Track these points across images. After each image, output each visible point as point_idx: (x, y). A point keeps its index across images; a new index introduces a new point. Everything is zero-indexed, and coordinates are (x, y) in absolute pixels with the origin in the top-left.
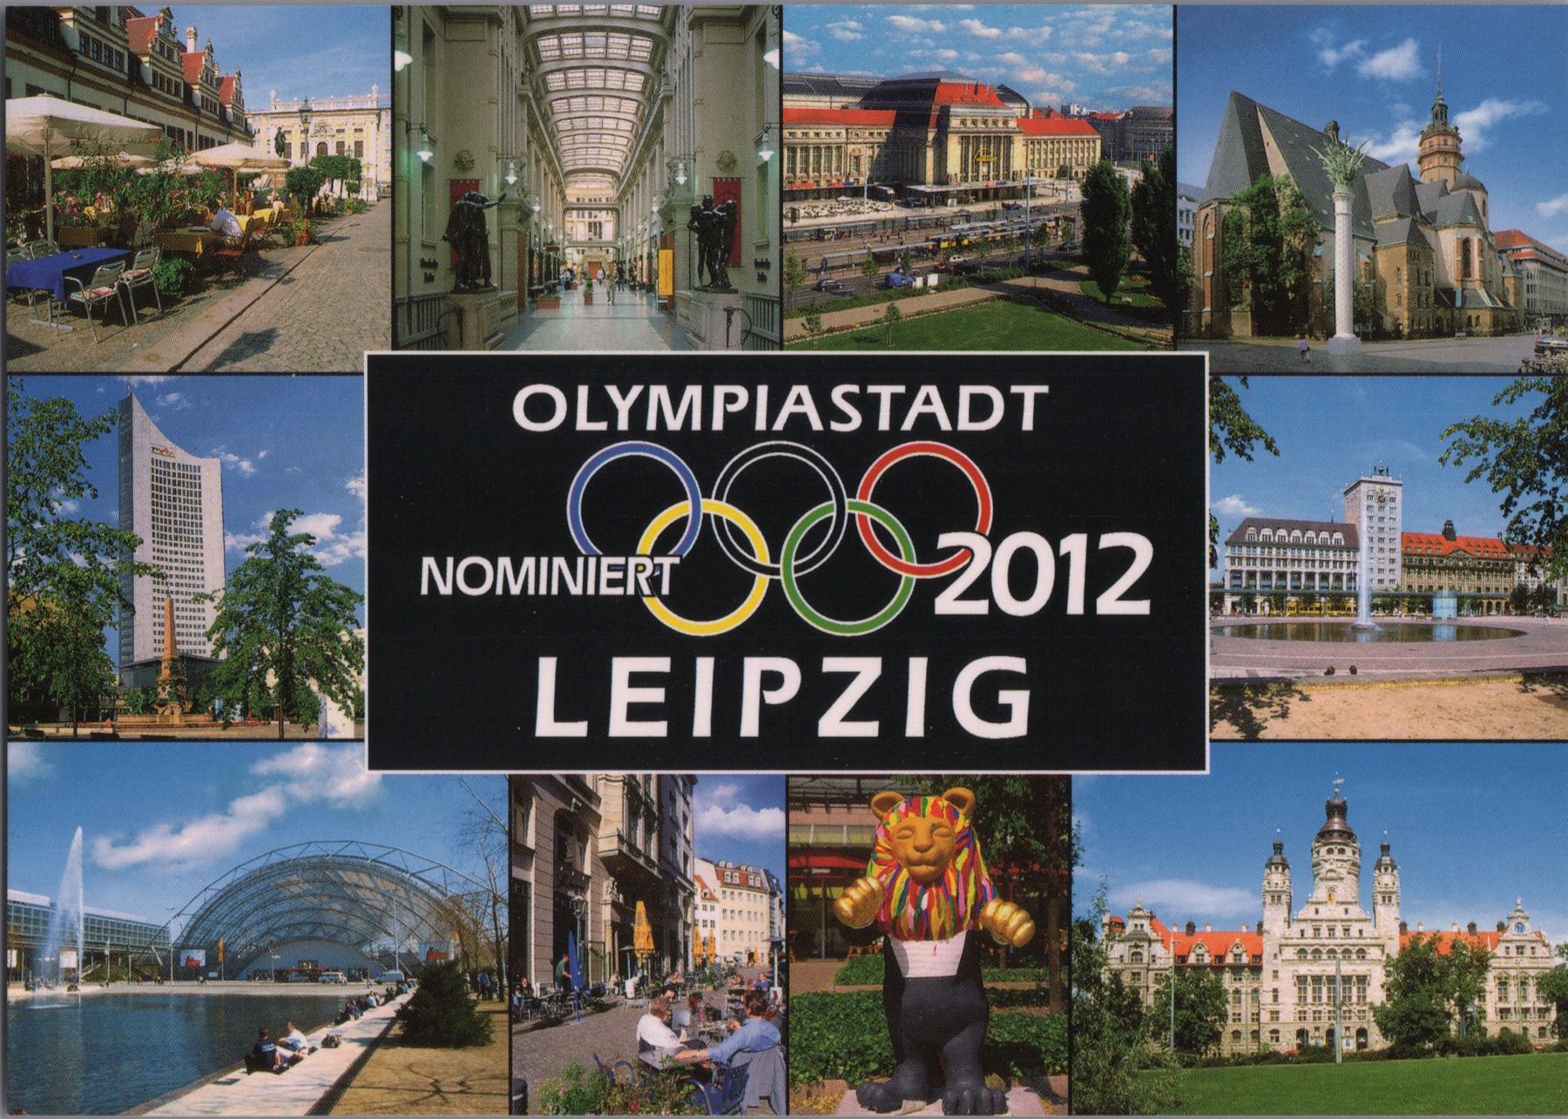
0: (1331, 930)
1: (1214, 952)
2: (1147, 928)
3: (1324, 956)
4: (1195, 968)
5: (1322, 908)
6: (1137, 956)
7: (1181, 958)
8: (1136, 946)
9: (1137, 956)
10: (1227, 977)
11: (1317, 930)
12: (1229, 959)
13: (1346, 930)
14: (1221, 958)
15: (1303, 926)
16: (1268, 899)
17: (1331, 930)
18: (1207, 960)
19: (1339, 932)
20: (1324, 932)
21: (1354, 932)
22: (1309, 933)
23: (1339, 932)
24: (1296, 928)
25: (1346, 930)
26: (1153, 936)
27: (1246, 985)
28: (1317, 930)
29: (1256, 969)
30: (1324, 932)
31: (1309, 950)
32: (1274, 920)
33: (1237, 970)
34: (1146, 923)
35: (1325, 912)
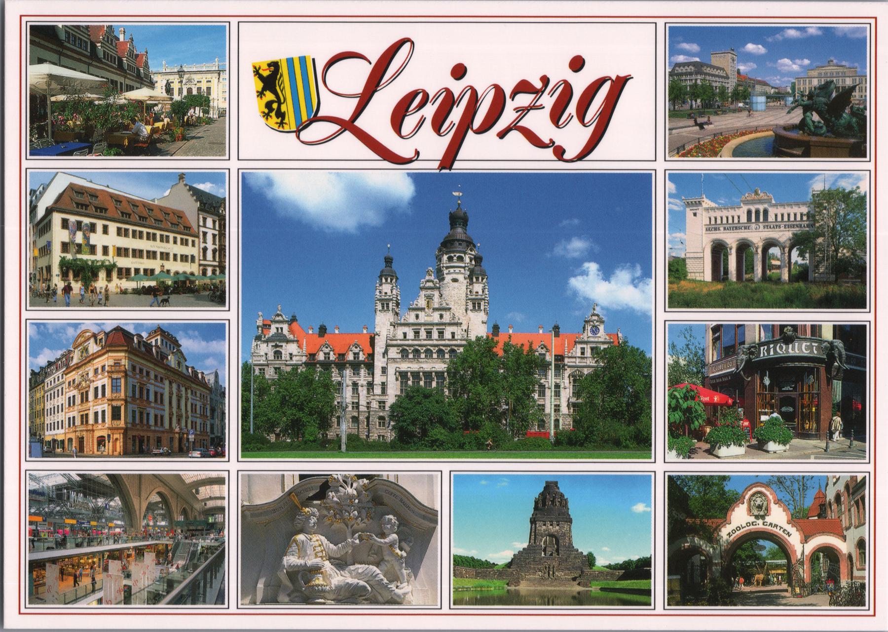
0: (429, 333)
1: (338, 351)
2: (286, 331)
3: (423, 356)
4: (322, 364)
5: (422, 314)
6: (278, 354)
7: (312, 356)
8: (276, 346)
9: (278, 354)
10: (348, 372)
11: (417, 333)
12: (350, 357)
13: (441, 333)
14: (342, 356)
15: (406, 329)
16: (379, 307)
17: (429, 333)
18: (332, 357)
19: (435, 335)
20: (423, 334)
21: (447, 335)
22: (411, 335)
23: (435, 335)
24: (400, 331)
25: (441, 333)
26: (291, 337)
27: (363, 378)
28: (417, 333)
29: (370, 366)
30: (423, 334)
31: (410, 350)
32: (383, 323)
33: (356, 366)
34: (285, 327)
35: (423, 318)
